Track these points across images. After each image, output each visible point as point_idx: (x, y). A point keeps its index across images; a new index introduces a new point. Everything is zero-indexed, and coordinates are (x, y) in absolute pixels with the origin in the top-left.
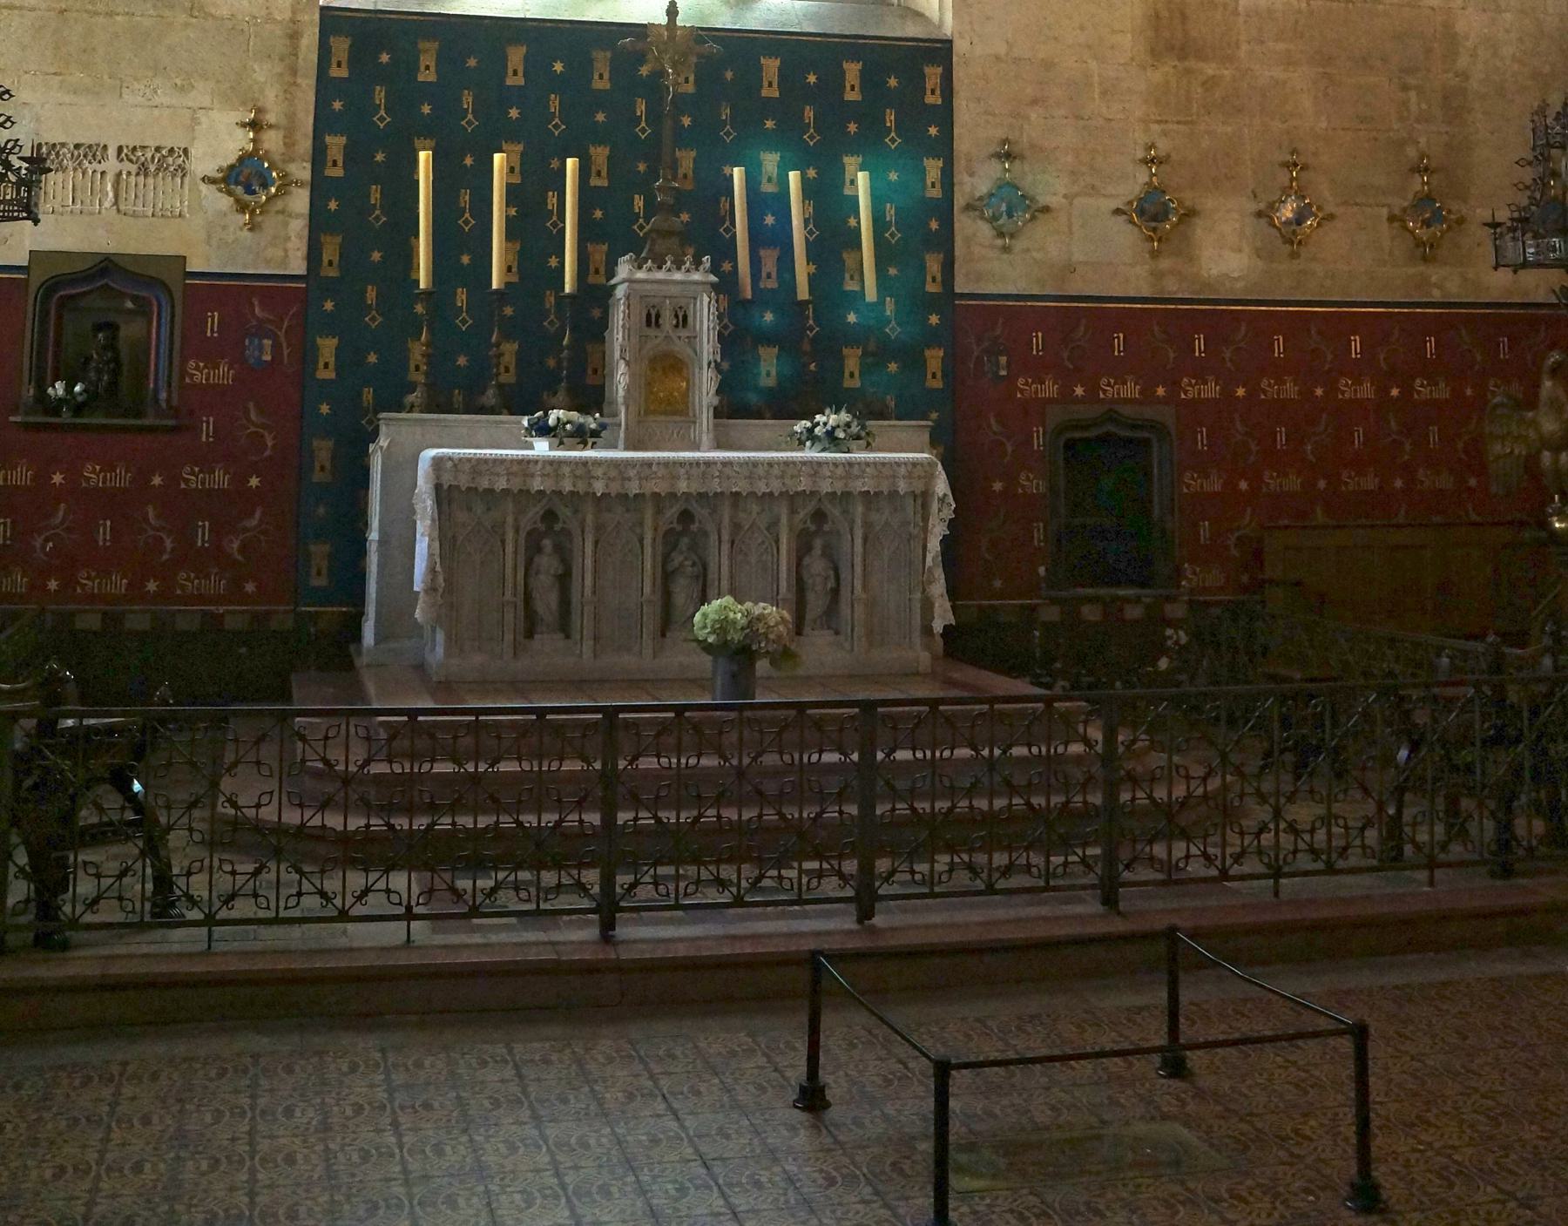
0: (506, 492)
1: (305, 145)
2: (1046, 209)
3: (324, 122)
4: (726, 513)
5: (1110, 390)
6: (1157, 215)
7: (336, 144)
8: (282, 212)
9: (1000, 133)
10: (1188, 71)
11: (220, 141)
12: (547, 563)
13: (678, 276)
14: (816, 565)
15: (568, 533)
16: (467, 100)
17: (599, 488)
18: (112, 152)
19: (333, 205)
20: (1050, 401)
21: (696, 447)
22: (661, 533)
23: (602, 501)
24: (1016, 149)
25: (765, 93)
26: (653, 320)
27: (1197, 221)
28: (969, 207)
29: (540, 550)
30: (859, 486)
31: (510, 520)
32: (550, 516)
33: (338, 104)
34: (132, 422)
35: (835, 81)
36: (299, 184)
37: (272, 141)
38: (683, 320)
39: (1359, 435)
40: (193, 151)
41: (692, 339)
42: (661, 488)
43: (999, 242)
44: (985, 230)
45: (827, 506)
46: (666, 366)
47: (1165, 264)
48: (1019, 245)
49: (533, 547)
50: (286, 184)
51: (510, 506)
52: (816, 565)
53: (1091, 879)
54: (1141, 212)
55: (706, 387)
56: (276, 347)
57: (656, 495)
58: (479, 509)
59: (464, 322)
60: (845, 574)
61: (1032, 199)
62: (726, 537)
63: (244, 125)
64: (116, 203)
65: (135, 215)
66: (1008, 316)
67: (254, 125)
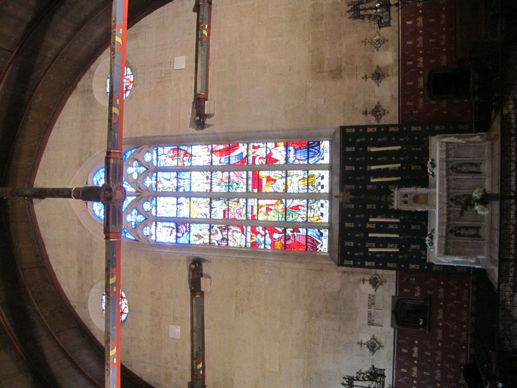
0: (446, 241)
1: (368, 270)
2: (378, 103)
3: (363, 266)
4: (451, 191)
5: (421, 85)
6: (378, 75)
7: (367, 264)
8: (382, 276)
9: (361, 114)
10: (344, 69)
11: (367, 288)
12: (462, 232)
13: (396, 197)
14: (464, 168)
15: (455, 228)
16: (357, 235)
17: (445, 220)
18: (370, 310)
19: (381, 264)
21: (435, 193)
22: (456, 206)
23: (449, 219)
24: (364, 110)
25: (353, 245)
26: (406, 202)
27: (380, 66)
28: (378, 122)
29: (459, 233)
30: (444, 159)
31: (452, 240)
32: (451, 231)
35: (350, 153)
37: (367, 277)
38: (406, 196)
40: (369, 293)
41: (410, 194)
42: (445, 206)
43: (386, 114)
44: (383, 118)
45: (450, 167)
46: (416, 199)
47: (390, 73)
48: (387, 109)
49: (459, 235)
50: (376, 274)
51: (449, 241)
52: (464, 168)
54: (378, 79)
55: (421, 190)
56: (413, 277)
57: (448, 207)
58: (449, 247)
59: (406, 256)
60: (466, 162)
61: (376, 106)
62: (457, 191)
63: (363, 283)
64: (380, 310)
66: (403, 109)
67: (363, 281)
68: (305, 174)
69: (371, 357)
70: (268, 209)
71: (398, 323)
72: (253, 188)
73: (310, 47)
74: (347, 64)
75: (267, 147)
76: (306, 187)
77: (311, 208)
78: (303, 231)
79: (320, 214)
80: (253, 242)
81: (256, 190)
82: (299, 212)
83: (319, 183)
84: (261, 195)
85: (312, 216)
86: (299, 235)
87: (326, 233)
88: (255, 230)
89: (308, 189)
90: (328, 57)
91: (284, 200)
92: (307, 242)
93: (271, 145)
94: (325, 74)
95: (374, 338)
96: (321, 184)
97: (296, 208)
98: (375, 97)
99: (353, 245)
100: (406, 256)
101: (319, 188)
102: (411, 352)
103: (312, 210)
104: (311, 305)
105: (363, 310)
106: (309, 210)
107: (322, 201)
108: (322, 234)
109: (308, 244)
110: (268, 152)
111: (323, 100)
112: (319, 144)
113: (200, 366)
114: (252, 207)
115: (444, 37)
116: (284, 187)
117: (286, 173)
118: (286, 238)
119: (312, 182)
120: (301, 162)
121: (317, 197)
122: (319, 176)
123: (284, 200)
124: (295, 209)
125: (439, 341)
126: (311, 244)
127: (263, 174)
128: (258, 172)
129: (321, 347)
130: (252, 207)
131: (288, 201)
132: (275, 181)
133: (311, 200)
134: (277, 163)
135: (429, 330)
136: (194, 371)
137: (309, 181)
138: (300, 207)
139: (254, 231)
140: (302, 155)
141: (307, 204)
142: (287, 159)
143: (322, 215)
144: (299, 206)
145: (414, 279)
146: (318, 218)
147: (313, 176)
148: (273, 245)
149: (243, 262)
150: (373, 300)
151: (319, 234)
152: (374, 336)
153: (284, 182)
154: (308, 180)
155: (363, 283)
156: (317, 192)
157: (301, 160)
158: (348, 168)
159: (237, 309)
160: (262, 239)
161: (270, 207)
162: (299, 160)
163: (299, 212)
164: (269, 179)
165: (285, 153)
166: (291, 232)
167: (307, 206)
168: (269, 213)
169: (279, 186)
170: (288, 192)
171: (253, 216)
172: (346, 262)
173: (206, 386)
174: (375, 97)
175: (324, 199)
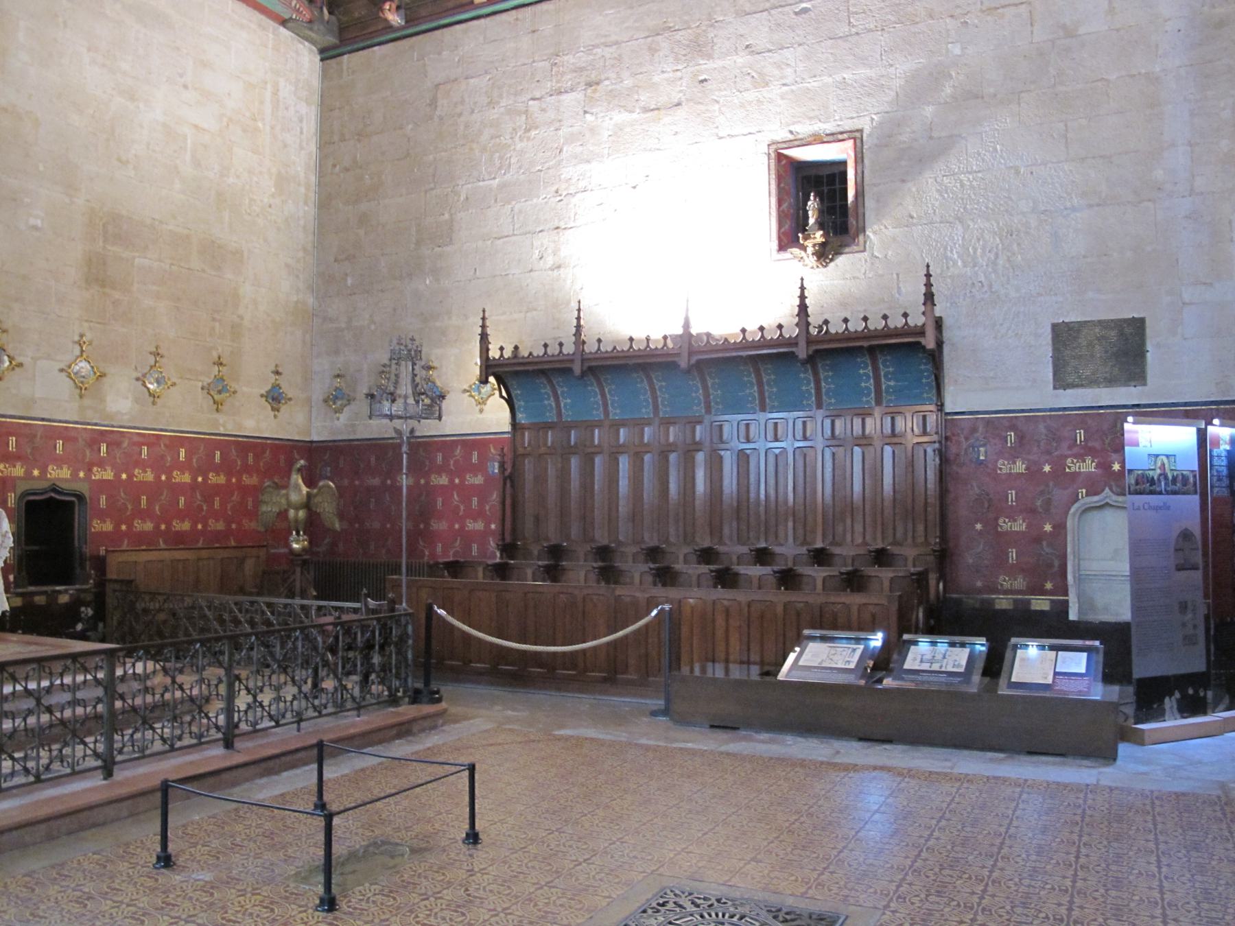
20: (19, 478)
39: (182, 500)
47: (87, 402)
53: (220, 735)
73: (161, 222)
74: (116, 303)
90: (137, 260)
94: (101, 244)
98: (35, 359)
111: (39, 223)
115: (148, 526)
174: (35, 359)
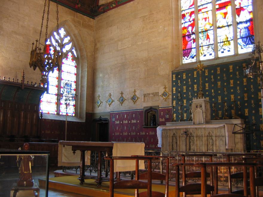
3: (173, 86)
7: (174, 89)
8: (168, 99)
11: (161, 91)
19: (174, 97)
33: (175, 84)
34: (155, 126)
36: (170, 95)
40: (159, 92)
56: (169, 116)
63: (164, 88)
65: (154, 101)
68: (231, 38)
69: (129, 98)
70: (205, 19)
71: (146, 111)
72: (218, 4)
75: (248, 6)
76: (222, 41)
77: (208, 48)
78: (194, 45)
79: (205, 54)
80: (185, 15)
81: (217, 7)
82: (205, 40)
83: (224, 50)
84: (215, 10)
85: (203, 49)
86: (191, 44)
87: (194, 60)
88: (192, 14)
89: (221, 42)
91: (212, 28)
92: (188, 49)
93: (250, 8)
95: (138, 98)
96: (224, 51)
97: (208, 37)
99: (184, 78)
100: (180, 111)
101: (222, 50)
102: (133, 119)
103: (207, 49)
104: (150, 60)
105: (151, 90)
106: (207, 46)
107: (213, 54)
108: (193, 58)
109: (187, 51)
110: (244, 8)
112: (252, 43)
113: (114, 6)
114: (207, 7)
116: (220, 26)
117: (231, 25)
118: (189, 36)
119: (225, 44)
120: (238, 34)
121: (216, 50)
122: (230, 49)
123: (212, 28)
124: (207, 36)
125: (140, 133)
126: (187, 53)
127: (229, 9)
128: (230, 5)
129: (132, 70)
130: (207, 7)
131: (212, 31)
132: (225, 18)
133: (213, 46)
134: (237, 16)
135: (144, 127)
136: (111, 3)
137: (226, 42)
138: (208, 40)
139: (192, 13)
140: (244, 33)
141: (211, 45)
142: (241, 23)
143: (205, 55)
144: (209, 39)
145: (168, 117)
146: (203, 53)
147: (229, 44)
148: (185, 28)
149: (169, 12)
150: (156, 95)
151: (193, 56)
152: (139, 98)
153: (224, 25)
154: (226, 41)
155: (164, 88)
156: (219, 49)
157: (240, 33)
158: (231, 67)
159: (145, 16)
160: (187, 20)
161: (207, 19)
162: (240, 32)
163: (205, 40)
164: (226, 14)
165: (244, 20)
166: (193, 38)
167: (209, 45)
168: (204, 20)
169: (221, 22)
170: (218, 30)
171: (200, 10)
172: (174, 76)
173: (107, 12)
175: (215, 55)
